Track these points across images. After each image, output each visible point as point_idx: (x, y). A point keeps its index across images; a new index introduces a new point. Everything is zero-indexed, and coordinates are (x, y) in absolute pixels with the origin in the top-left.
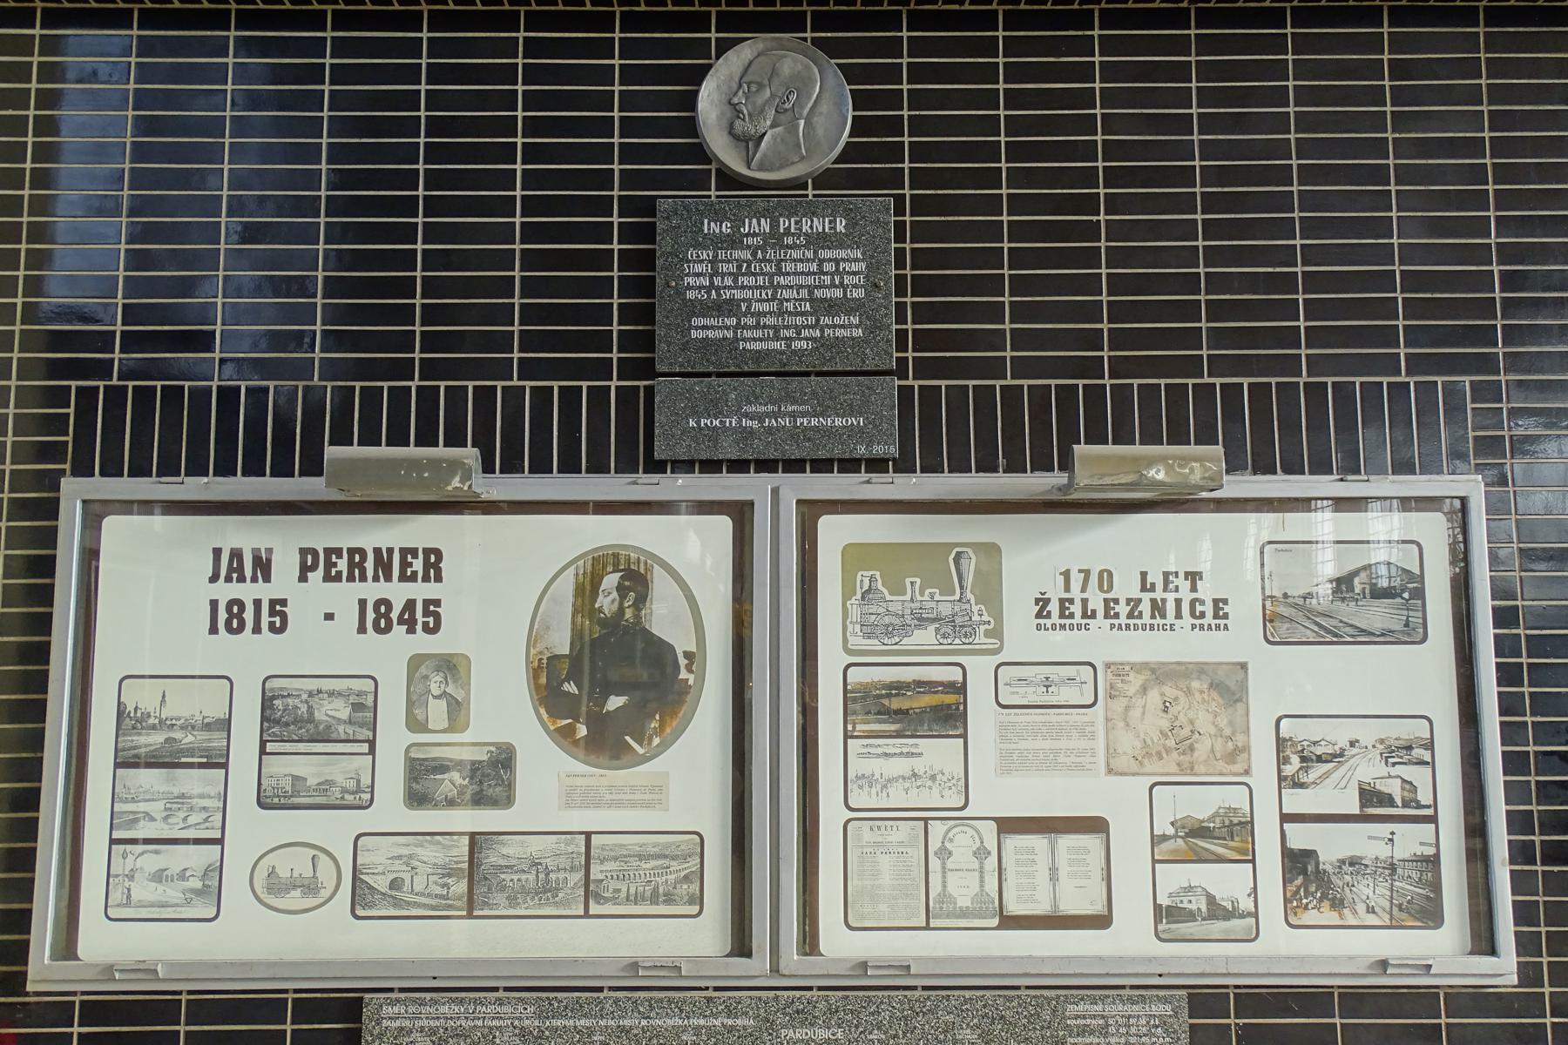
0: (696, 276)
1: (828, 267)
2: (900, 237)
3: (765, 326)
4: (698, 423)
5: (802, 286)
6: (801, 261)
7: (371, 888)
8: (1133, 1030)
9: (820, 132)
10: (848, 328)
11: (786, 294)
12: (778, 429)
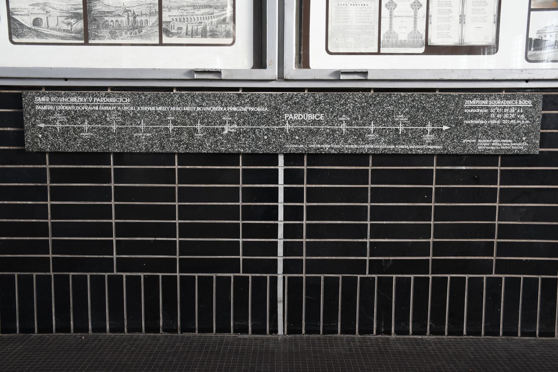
7: (21, 24)
8: (506, 116)
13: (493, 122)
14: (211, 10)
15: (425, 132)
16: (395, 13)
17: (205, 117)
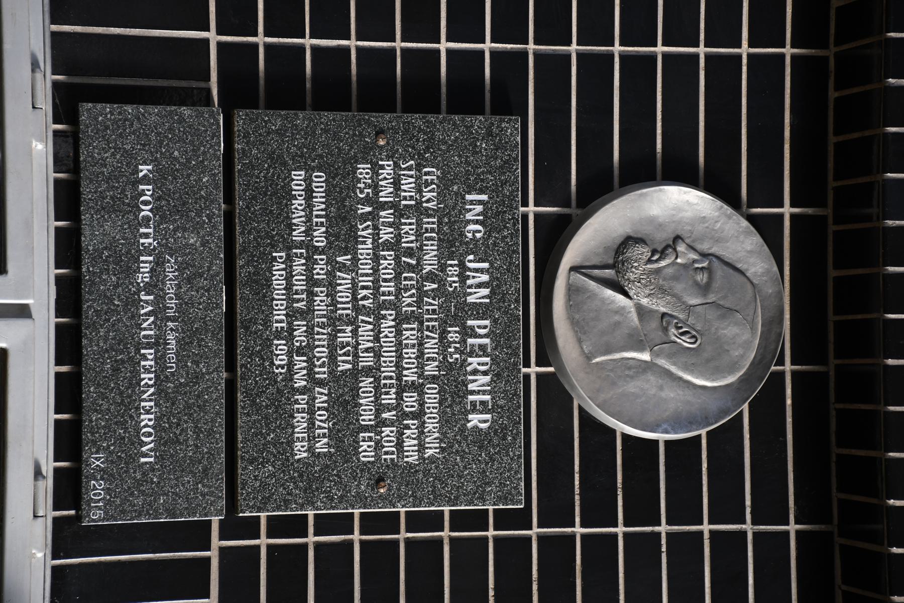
0: (395, 179)
1: (410, 400)
2: (460, 520)
3: (311, 294)
4: (145, 180)
5: (378, 355)
6: (420, 355)
9: (632, 387)
10: (308, 435)
11: (365, 331)
12: (135, 316)
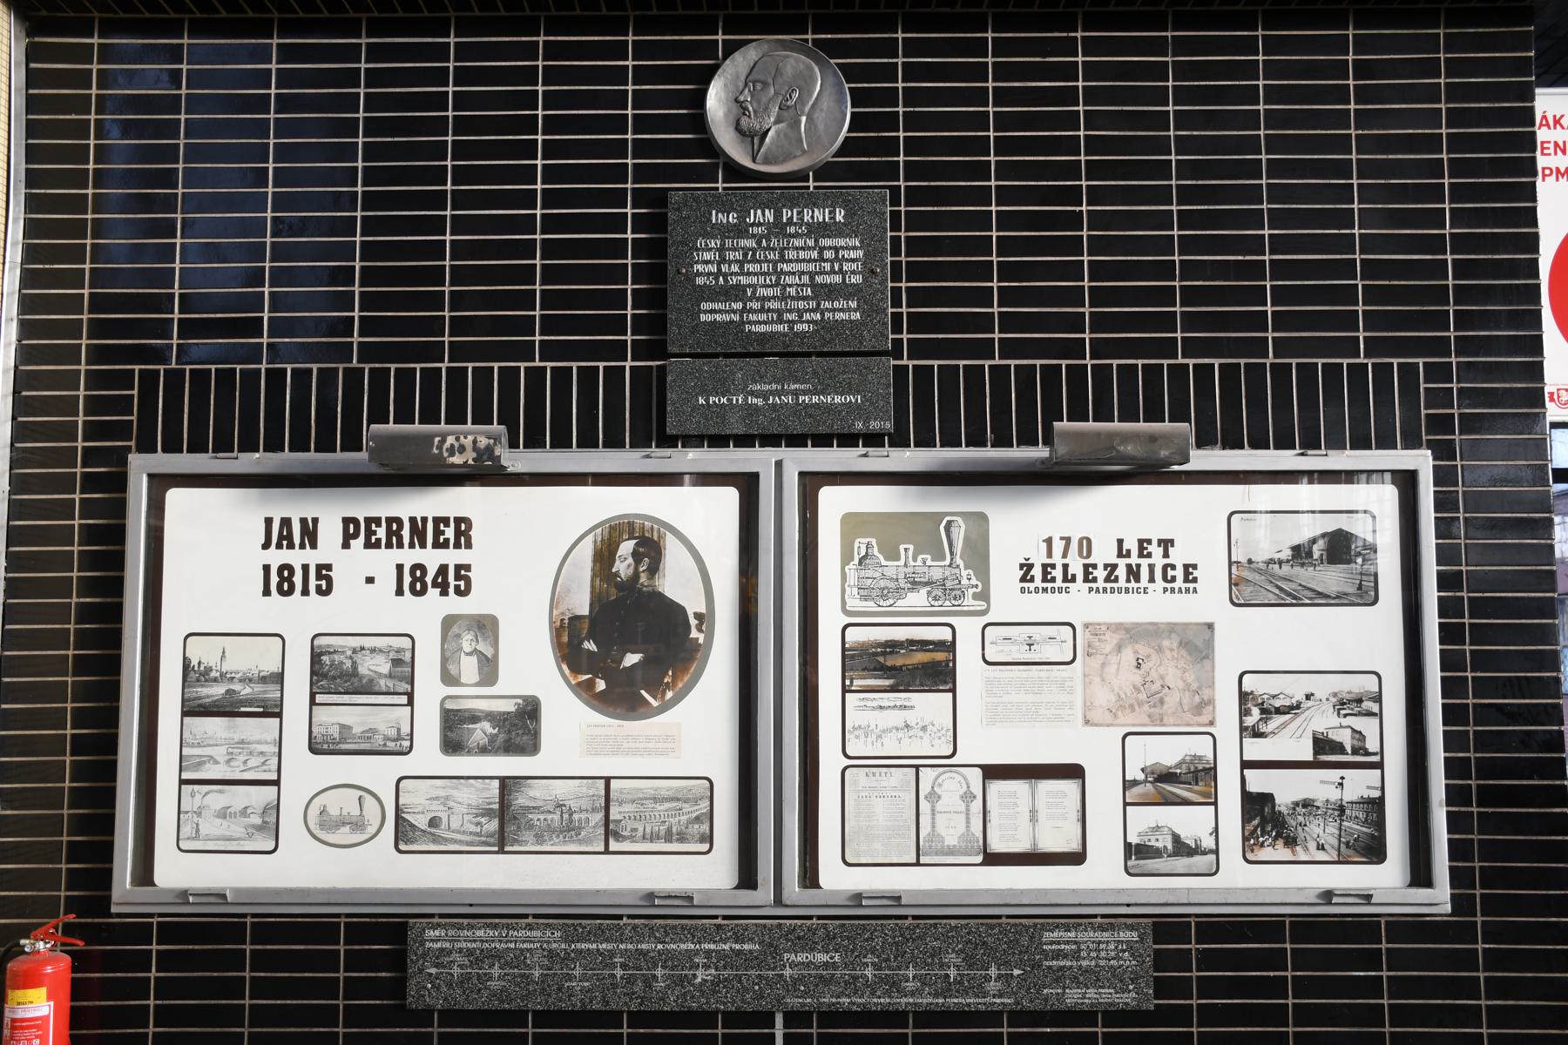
0: (704, 264)
1: (828, 254)
2: (895, 226)
3: (769, 310)
4: (707, 400)
5: (803, 273)
6: (803, 249)
7: (412, 825)
8: (1103, 954)
9: (821, 127)
10: (847, 312)
11: (789, 280)
12: (781, 406)
13: (1085, 963)
14: (679, 805)
15: (987, 978)
16: (939, 807)
17: (668, 959)
